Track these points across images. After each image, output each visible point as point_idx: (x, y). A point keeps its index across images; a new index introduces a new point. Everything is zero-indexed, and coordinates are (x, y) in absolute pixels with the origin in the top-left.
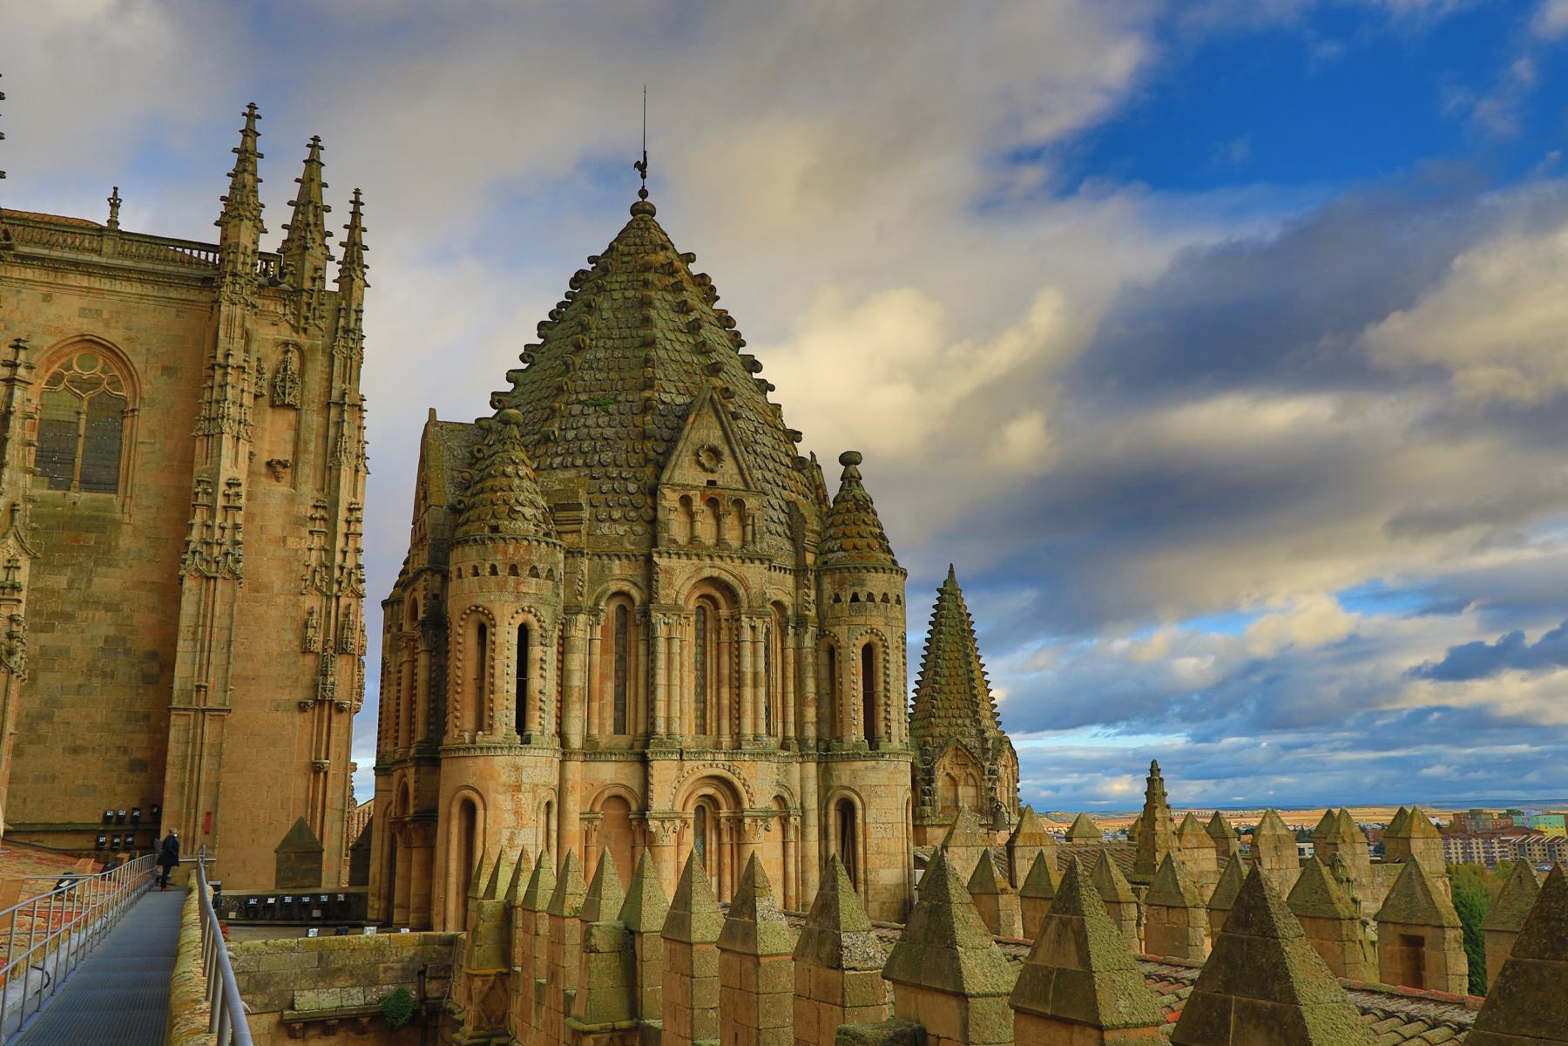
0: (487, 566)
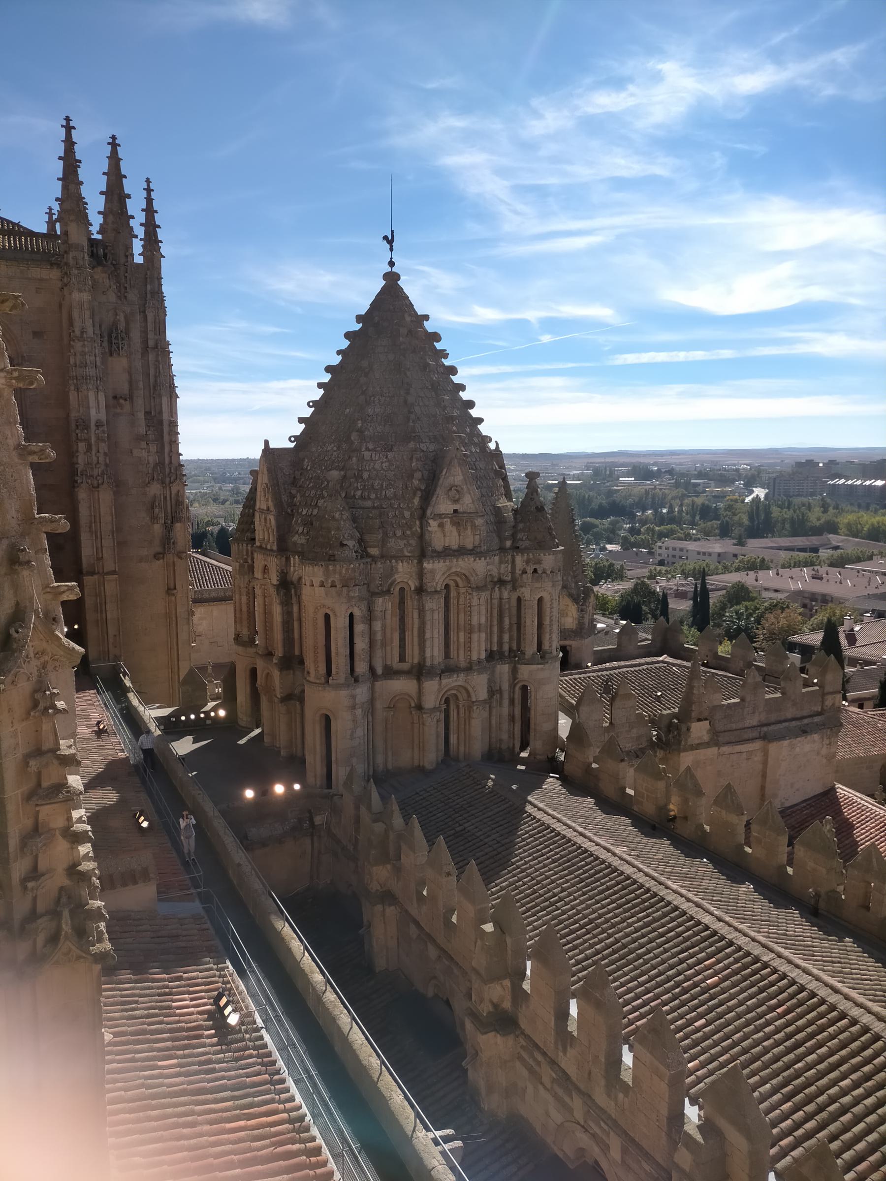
0: (329, 581)
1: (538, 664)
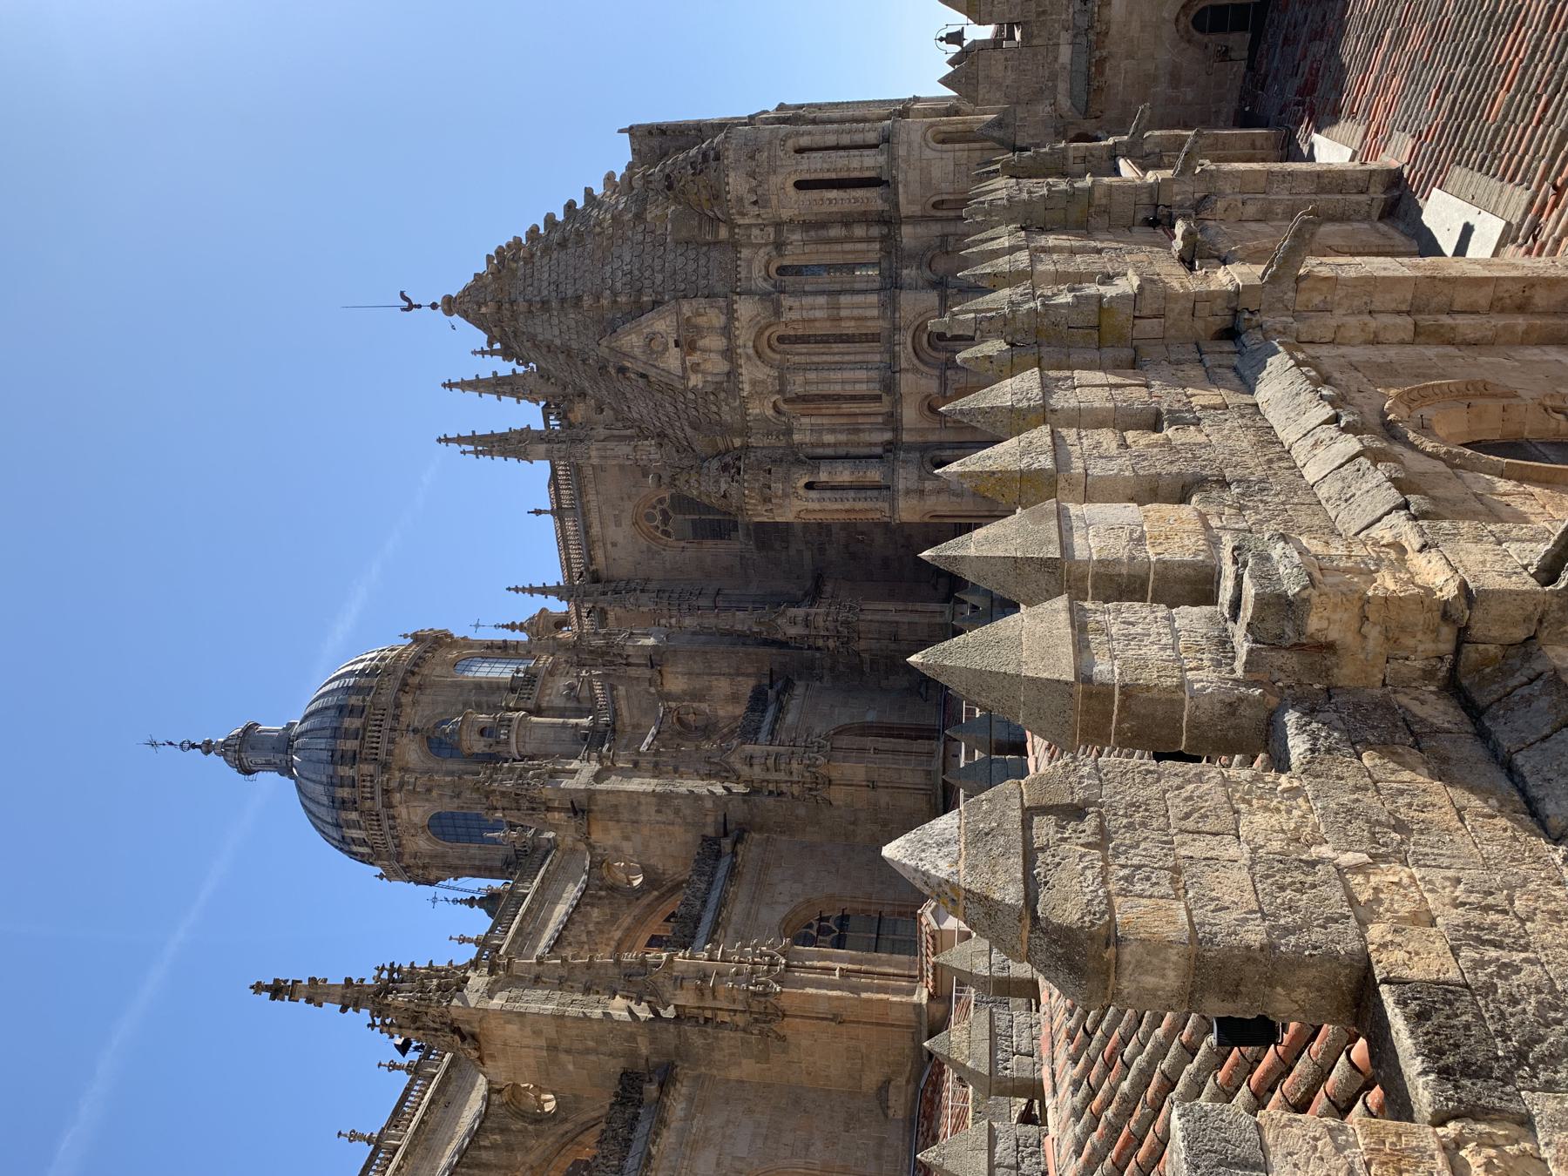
1: (896, 194)
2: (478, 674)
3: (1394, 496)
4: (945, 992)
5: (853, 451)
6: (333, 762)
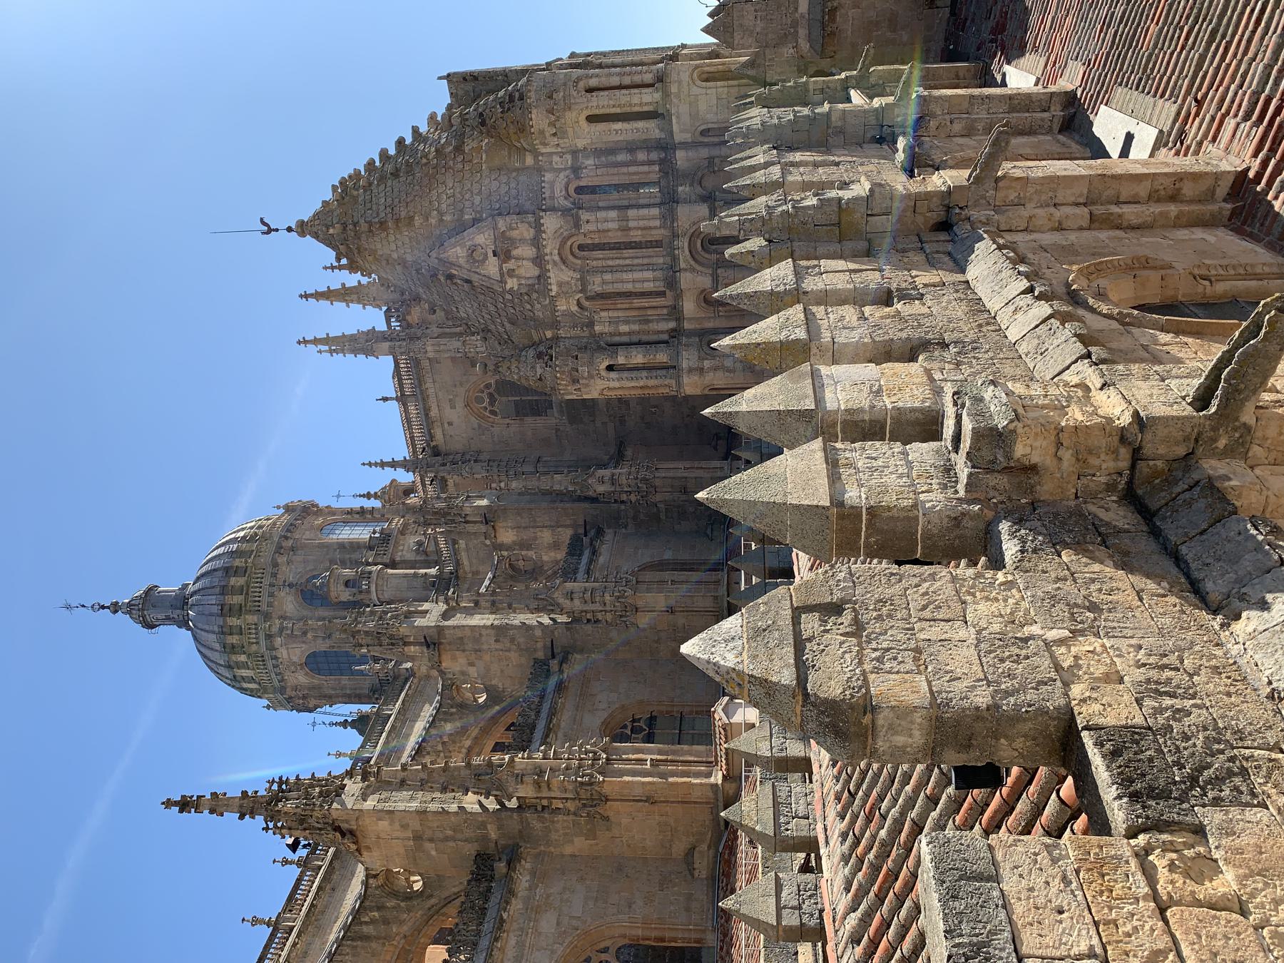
1: (671, 124)
2: (341, 536)
3: (1079, 348)
4: (736, 773)
5: (645, 338)
6: (222, 615)
